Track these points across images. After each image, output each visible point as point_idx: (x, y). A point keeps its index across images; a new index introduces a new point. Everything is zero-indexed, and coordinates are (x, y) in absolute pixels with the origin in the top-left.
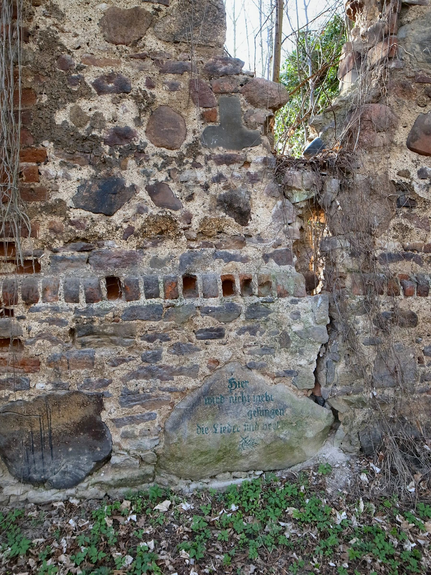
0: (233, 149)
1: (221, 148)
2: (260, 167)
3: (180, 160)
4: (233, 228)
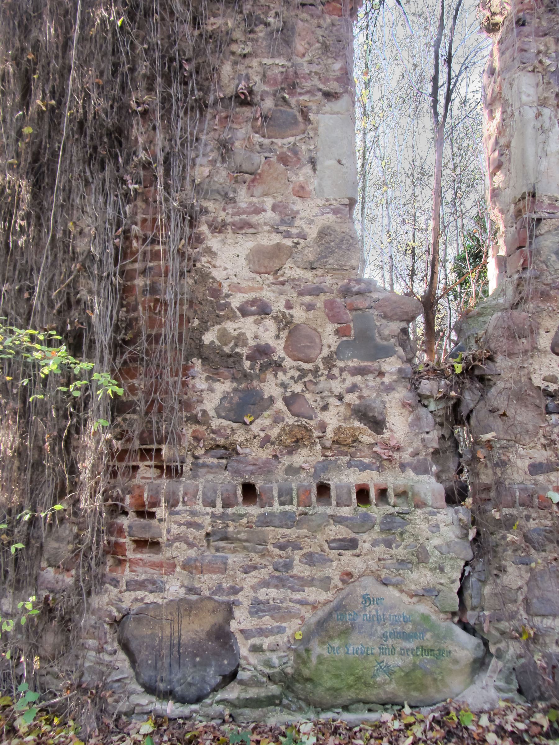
0: (368, 360)
1: (355, 360)
2: (395, 377)
3: (315, 372)
4: (367, 437)
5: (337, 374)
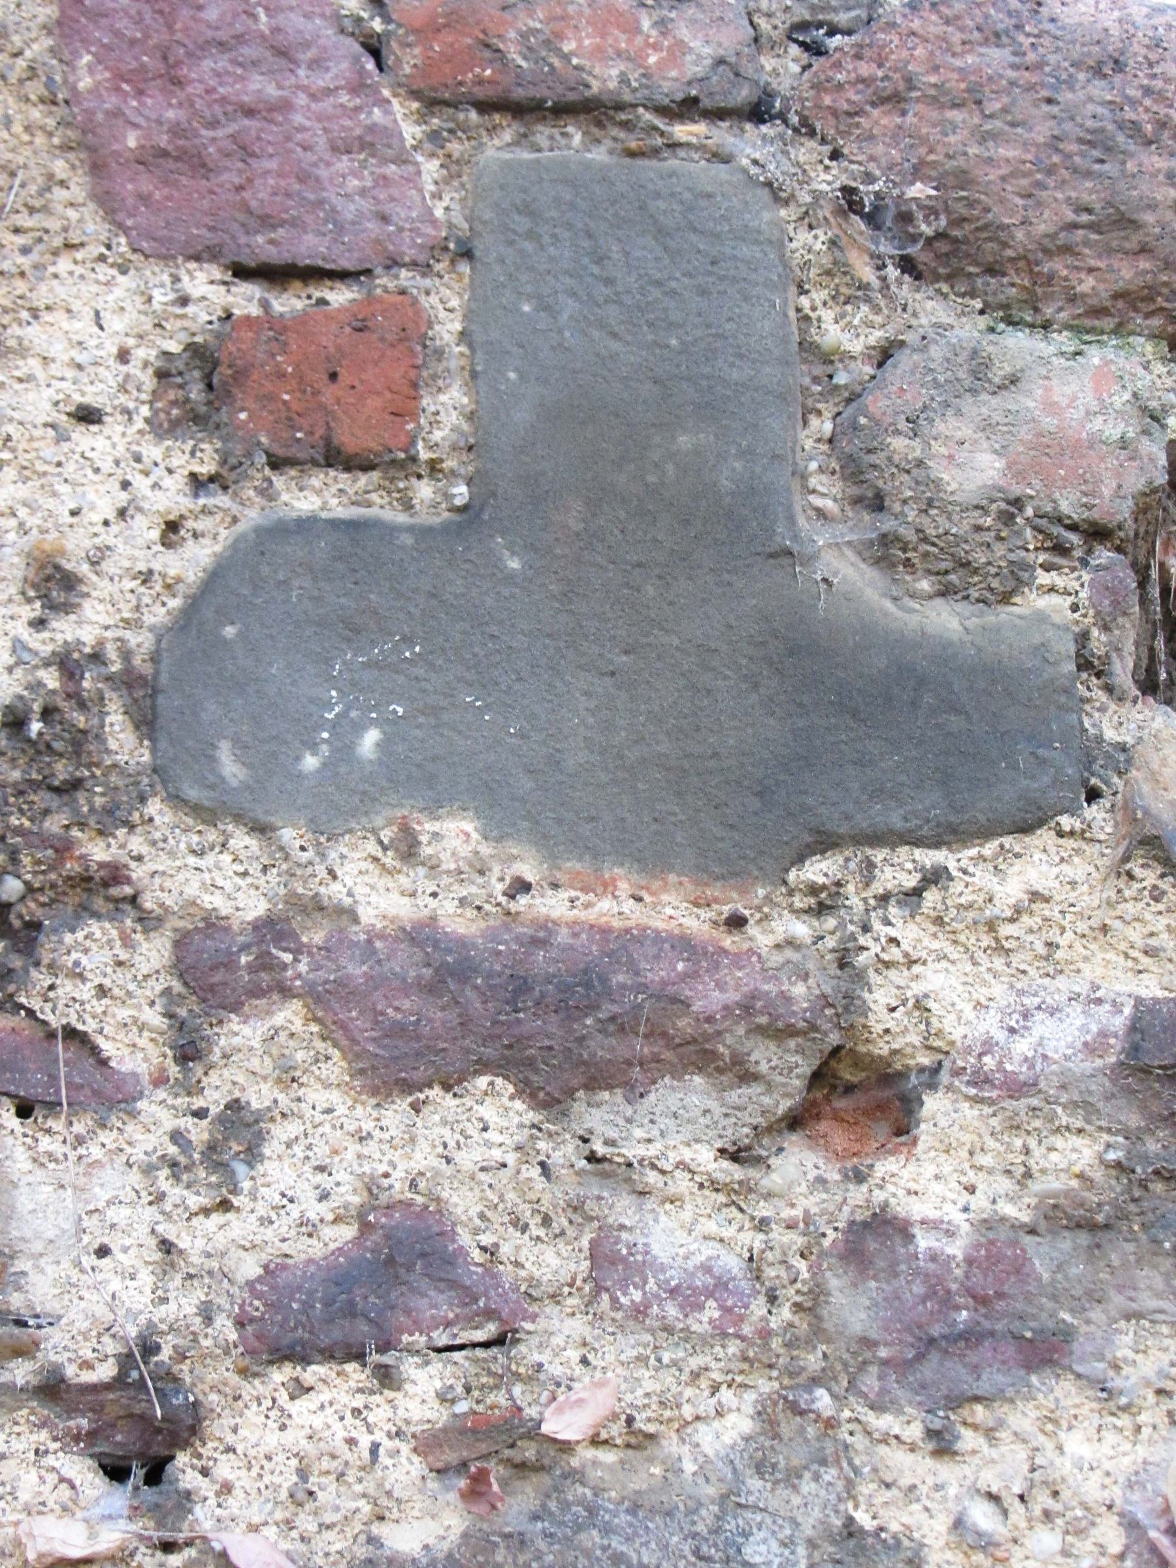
0: (653, 861)
1: (454, 835)
2: (1073, 1157)
5: (132, 1043)
